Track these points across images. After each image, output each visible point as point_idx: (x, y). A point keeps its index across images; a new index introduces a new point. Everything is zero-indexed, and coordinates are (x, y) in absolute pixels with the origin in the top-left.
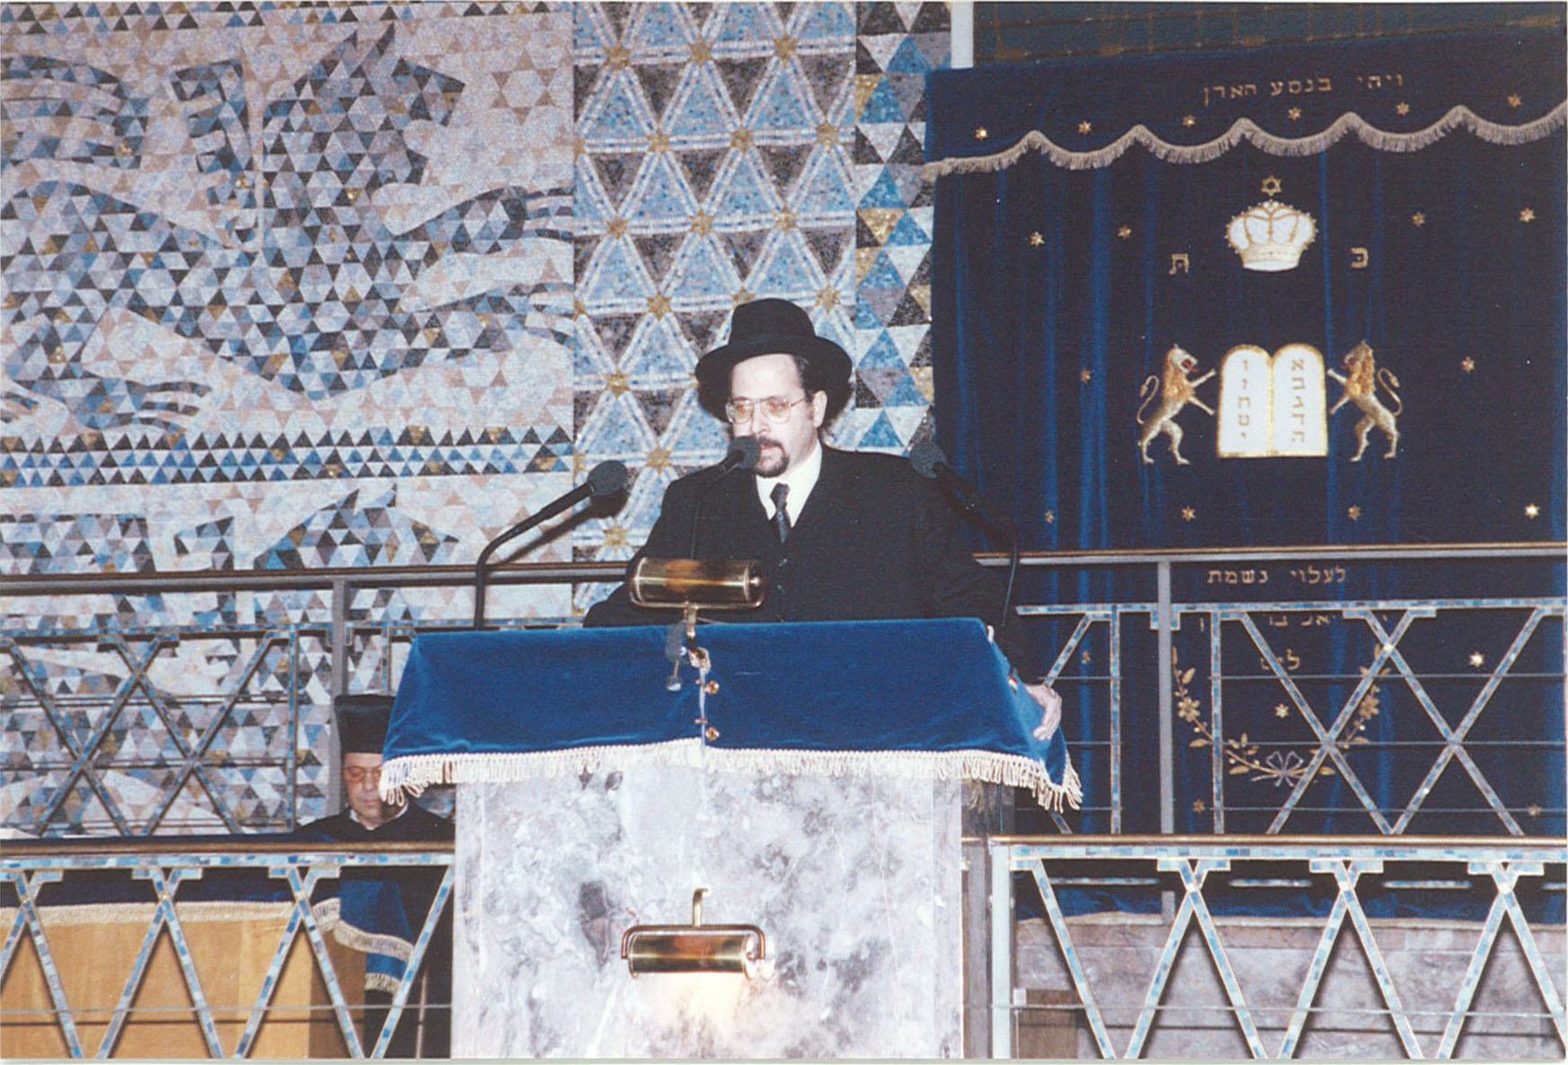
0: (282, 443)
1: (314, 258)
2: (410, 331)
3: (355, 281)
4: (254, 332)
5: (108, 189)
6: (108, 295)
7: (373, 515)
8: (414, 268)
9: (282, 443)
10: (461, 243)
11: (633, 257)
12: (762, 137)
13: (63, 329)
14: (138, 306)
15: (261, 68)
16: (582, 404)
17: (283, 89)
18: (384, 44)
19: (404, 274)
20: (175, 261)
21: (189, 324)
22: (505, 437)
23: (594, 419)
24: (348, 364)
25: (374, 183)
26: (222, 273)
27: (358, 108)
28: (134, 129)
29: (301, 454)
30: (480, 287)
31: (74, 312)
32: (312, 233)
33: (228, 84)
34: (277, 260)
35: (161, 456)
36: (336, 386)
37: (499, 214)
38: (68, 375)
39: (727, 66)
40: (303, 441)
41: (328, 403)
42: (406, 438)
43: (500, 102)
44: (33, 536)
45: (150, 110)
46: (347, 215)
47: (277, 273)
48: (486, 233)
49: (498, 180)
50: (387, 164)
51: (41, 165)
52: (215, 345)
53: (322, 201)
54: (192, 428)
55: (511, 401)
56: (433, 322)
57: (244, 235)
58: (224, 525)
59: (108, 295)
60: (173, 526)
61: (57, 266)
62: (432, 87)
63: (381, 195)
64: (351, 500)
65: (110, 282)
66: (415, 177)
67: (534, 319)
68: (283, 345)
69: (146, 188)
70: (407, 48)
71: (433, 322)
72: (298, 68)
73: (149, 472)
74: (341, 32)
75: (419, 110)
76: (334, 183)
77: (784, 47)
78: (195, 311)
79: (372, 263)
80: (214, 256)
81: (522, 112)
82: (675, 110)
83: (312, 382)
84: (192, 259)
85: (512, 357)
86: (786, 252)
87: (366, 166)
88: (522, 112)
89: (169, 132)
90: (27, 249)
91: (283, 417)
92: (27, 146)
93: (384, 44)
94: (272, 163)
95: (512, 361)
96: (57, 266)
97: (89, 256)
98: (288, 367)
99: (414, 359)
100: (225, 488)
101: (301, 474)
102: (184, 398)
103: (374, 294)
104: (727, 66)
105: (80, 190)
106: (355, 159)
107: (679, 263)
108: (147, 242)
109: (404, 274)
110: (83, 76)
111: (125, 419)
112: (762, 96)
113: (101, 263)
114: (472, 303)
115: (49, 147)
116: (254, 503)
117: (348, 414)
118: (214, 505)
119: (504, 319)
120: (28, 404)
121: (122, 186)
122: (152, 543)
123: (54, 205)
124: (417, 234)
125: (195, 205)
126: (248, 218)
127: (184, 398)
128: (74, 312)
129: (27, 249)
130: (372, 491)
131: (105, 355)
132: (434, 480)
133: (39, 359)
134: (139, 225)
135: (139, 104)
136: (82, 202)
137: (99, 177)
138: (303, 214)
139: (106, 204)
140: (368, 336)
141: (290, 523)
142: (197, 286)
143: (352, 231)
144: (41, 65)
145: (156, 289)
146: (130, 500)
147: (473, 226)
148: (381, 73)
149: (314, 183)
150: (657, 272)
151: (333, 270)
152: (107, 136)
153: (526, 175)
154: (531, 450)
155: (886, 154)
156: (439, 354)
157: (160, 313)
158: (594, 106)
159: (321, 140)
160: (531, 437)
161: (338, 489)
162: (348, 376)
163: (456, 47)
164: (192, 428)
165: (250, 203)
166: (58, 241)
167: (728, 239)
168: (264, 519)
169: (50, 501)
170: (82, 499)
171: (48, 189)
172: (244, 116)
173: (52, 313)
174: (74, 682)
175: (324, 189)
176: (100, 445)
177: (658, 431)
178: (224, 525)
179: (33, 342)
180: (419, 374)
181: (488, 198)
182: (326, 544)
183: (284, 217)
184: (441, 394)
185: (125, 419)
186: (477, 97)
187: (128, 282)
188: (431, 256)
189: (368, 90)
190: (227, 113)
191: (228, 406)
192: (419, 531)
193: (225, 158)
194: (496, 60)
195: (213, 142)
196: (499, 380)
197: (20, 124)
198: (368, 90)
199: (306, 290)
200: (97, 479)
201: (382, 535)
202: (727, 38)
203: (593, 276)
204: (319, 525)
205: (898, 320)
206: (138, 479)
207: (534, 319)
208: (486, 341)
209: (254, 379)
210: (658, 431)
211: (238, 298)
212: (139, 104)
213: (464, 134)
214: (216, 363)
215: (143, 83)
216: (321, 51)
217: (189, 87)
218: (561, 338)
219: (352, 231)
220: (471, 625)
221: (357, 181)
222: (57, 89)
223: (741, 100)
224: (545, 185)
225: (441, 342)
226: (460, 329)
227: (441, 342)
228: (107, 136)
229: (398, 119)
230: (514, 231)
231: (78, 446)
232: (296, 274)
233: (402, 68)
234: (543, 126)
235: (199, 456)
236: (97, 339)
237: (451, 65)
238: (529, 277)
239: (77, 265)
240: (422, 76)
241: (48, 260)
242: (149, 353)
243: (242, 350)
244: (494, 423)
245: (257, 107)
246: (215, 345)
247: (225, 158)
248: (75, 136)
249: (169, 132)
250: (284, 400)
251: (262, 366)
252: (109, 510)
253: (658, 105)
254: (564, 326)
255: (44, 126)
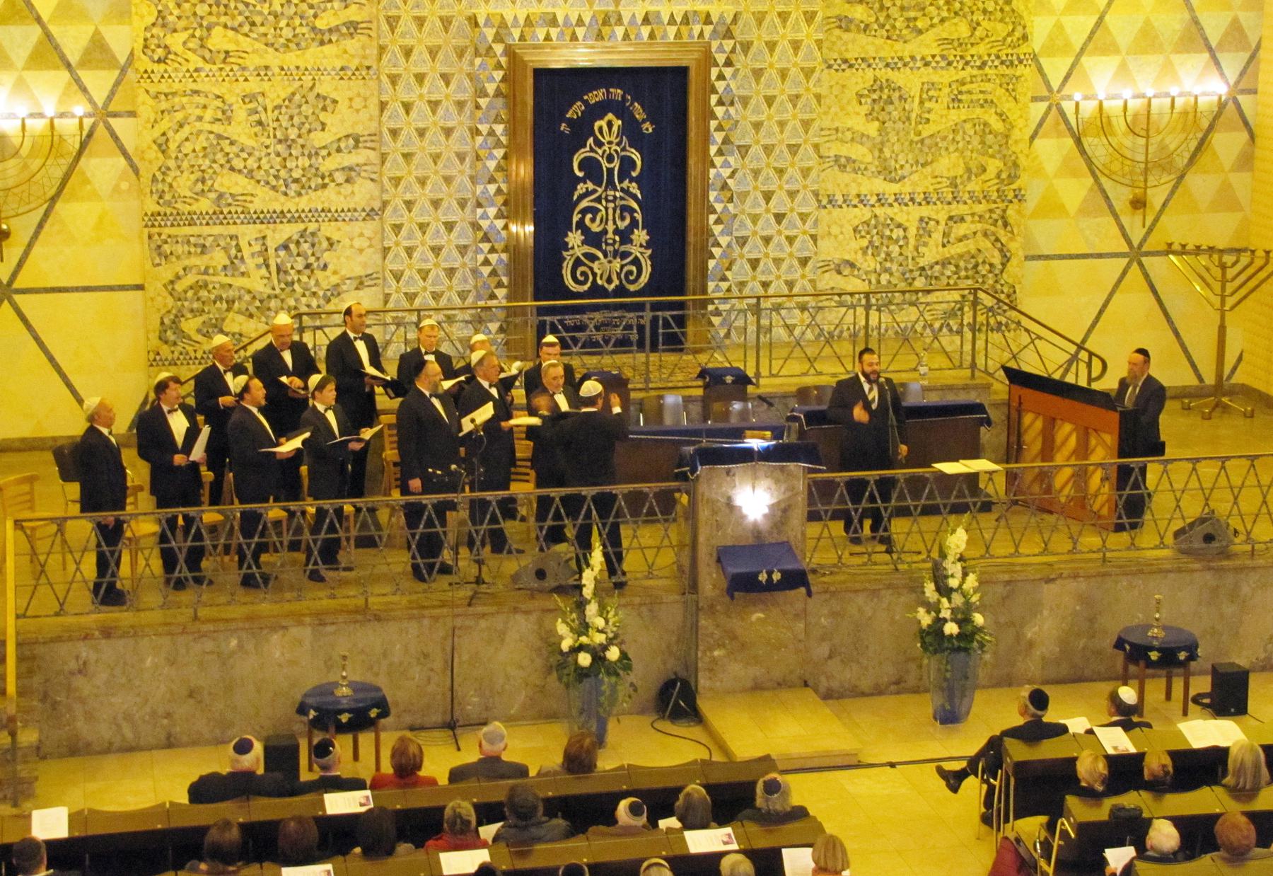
0: (282, 212)
1: (291, 154)
2: (323, 178)
3: (304, 162)
4: (271, 178)
5: (221, 132)
6: (222, 166)
7: (313, 234)
8: (323, 158)
9: (282, 212)
10: (339, 150)
11: (400, 159)
12: (442, 123)
13: (207, 176)
14: (232, 169)
15: (271, 95)
16: (385, 204)
17: (279, 102)
18: (311, 89)
19: (320, 160)
20: (244, 155)
21: (250, 175)
22: (355, 210)
23: (389, 209)
24: (303, 187)
25: (310, 131)
26: (260, 159)
27: (304, 107)
28: (229, 113)
29: (289, 215)
30: (346, 164)
31: (211, 171)
32: (290, 147)
33: (260, 99)
34: (278, 155)
35: (242, 216)
36: (299, 194)
37: (351, 142)
38: (210, 191)
39: (430, 102)
40: (289, 211)
41: (297, 199)
42: (323, 210)
43: (351, 107)
44: (202, 241)
45: (234, 107)
46: (301, 141)
47: (279, 159)
48: (347, 147)
49: (350, 131)
50: (313, 126)
51: (198, 124)
52: (258, 182)
53: (293, 137)
54: (252, 208)
55: (357, 198)
56: (330, 175)
57: (267, 147)
58: (264, 238)
59: (222, 166)
60: (247, 238)
61: (205, 156)
62: (328, 102)
63: (312, 135)
64: (305, 230)
65: (222, 161)
66: (323, 130)
67: (363, 174)
68: (281, 182)
69: (232, 131)
70: (321, 89)
71: (330, 175)
72: (283, 95)
73: (238, 221)
74: (297, 84)
75: (324, 109)
76: (296, 131)
77: (447, 96)
78: (251, 171)
79: (310, 156)
80: (257, 154)
81: (358, 111)
82: (413, 114)
83: (292, 193)
84: (250, 154)
85: (356, 186)
86: (449, 158)
87: (307, 126)
88: (358, 111)
89: (240, 113)
90: (194, 151)
91: (283, 204)
92: (192, 118)
93: (311, 89)
94: (276, 124)
95: (356, 188)
96: (205, 156)
97: (214, 154)
98: (283, 189)
99: (324, 186)
100: (264, 226)
101: (289, 221)
102: (249, 198)
103: (311, 166)
104: (430, 102)
105: (211, 132)
106: (303, 124)
107: (416, 160)
108: (235, 149)
109: (320, 160)
110: (210, 96)
111: (230, 205)
112: (440, 111)
113: (219, 156)
114: (343, 169)
115: (200, 118)
116: (274, 231)
117: (303, 203)
118: (260, 231)
119: (353, 174)
120: (197, 200)
121: (225, 131)
122: (241, 243)
123: (202, 137)
124: (324, 147)
125: (250, 137)
126: (268, 142)
127: (249, 198)
128: (211, 171)
129: (194, 151)
130: (312, 227)
131: (222, 185)
132: (333, 224)
133: (200, 186)
134: (232, 143)
135: (230, 105)
136: (212, 136)
137: (217, 128)
138: (286, 140)
139: (219, 137)
140: (309, 179)
141: (286, 237)
142: (251, 163)
143: (303, 146)
144: (196, 92)
145: (238, 164)
146: (232, 230)
147: (343, 145)
148: (311, 97)
149: (290, 131)
150: (408, 164)
151: (297, 158)
152: (220, 115)
153: (359, 130)
154: (364, 214)
155: (485, 133)
156: (333, 185)
157: (240, 171)
158: (386, 114)
159: (291, 118)
160: (364, 210)
161: (301, 226)
162: (303, 192)
163: (336, 89)
164: (252, 208)
165: (269, 137)
166: (205, 148)
167: (431, 155)
168: (277, 236)
169: (206, 230)
170: (217, 230)
171: (200, 132)
172: (265, 109)
173: (203, 171)
174: (217, 286)
175: (293, 134)
176: (222, 213)
177: (410, 211)
178: (264, 238)
179: (197, 180)
180: (326, 192)
181: (347, 136)
182: (298, 243)
183: (280, 141)
184: (333, 197)
185: (230, 205)
186: (343, 106)
187: (228, 161)
188: (329, 154)
189: (307, 102)
190: (260, 109)
191: (264, 200)
192: (328, 239)
193: (260, 123)
194: (350, 94)
195: (256, 117)
196: (353, 193)
197: (190, 111)
198: (307, 102)
199: (288, 164)
200: (221, 223)
201: (316, 240)
202: (429, 93)
203: (388, 164)
204: (295, 237)
205: (489, 182)
206: (235, 223)
207: (363, 174)
208: (347, 181)
209: (272, 193)
210: (410, 211)
211: (266, 167)
212: (230, 105)
213: (339, 116)
214: (259, 187)
215: (230, 99)
216: (290, 90)
217: (247, 100)
218: (372, 180)
219: (303, 146)
220: (748, 433)
221: (304, 131)
222: (201, 100)
223: (434, 112)
224: (366, 133)
225: (333, 181)
226: (340, 177)
227: (333, 181)
228: (220, 115)
229: (317, 111)
230: (356, 147)
231: (215, 213)
232: (285, 159)
233: (318, 95)
234: (364, 115)
235: (255, 216)
236: (219, 179)
237: (334, 95)
238: (361, 160)
239: (211, 156)
240: (325, 98)
241: (201, 155)
242: (237, 184)
243: (268, 183)
244: (352, 206)
245: (270, 108)
246: (258, 182)
247: (260, 123)
248: (208, 115)
249: (240, 113)
250: (283, 198)
251: (274, 188)
252: (226, 233)
253: (408, 113)
254: (373, 176)
255: (199, 112)
